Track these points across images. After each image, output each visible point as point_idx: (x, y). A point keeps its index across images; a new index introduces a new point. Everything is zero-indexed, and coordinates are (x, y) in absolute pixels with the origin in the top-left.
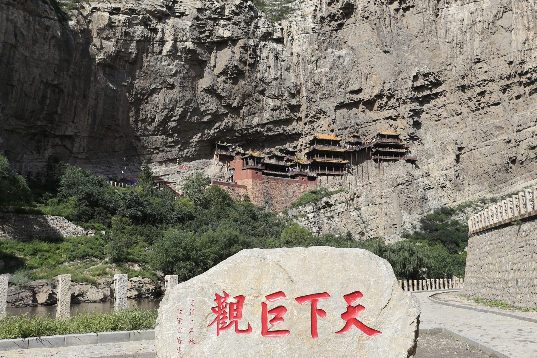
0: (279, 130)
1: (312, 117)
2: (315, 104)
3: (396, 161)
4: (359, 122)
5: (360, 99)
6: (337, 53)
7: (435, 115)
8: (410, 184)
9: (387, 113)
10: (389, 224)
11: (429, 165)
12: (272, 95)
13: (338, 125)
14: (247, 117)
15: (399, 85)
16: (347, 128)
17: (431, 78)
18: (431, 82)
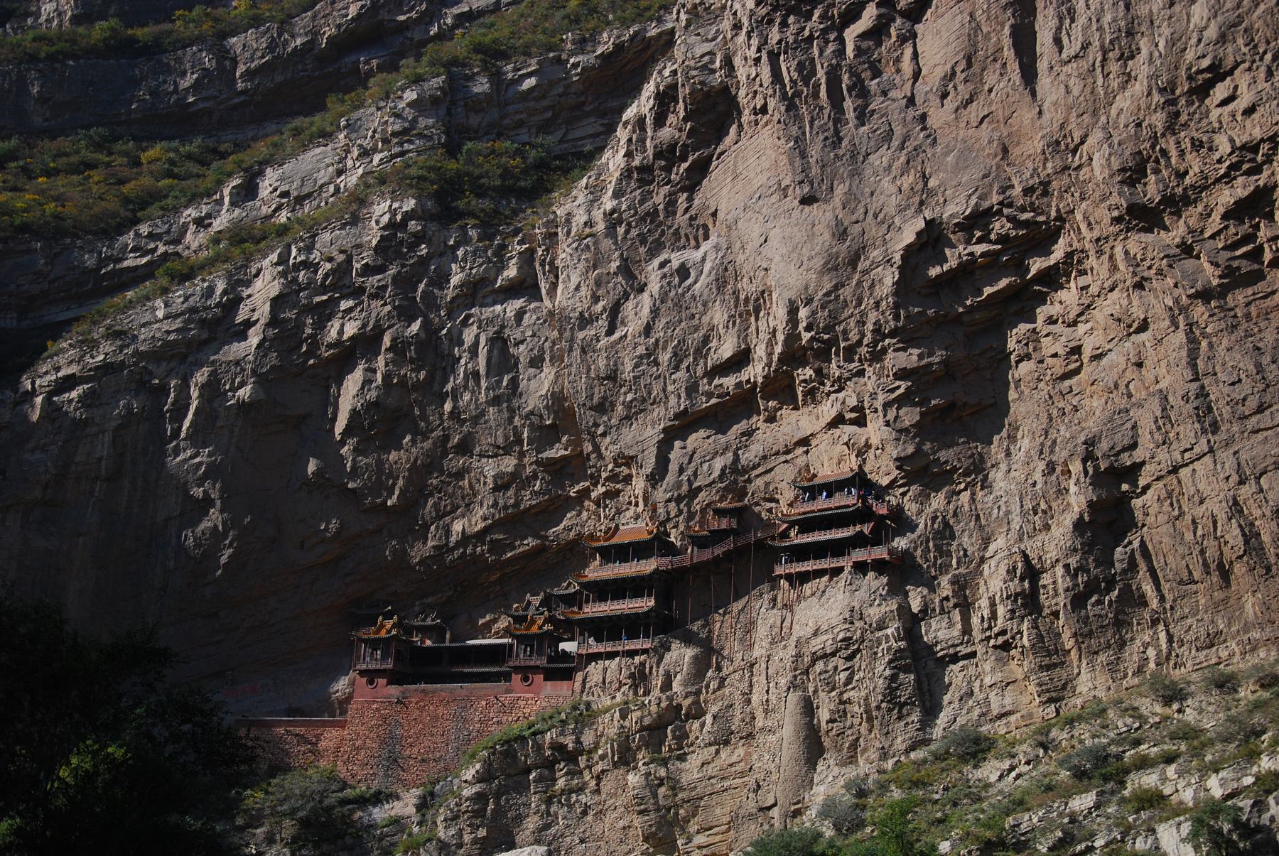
0: (525, 542)
1: (607, 479)
2: (608, 439)
3: (837, 571)
4: (747, 457)
5: (748, 381)
6: (676, 260)
7: (1055, 355)
8: (858, 650)
9: (828, 410)
10: (751, 806)
11: (986, 566)
12: (491, 448)
13: (664, 487)
14: (432, 524)
15: (849, 299)
16: (699, 489)
17: (999, 226)
18: (1003, 239)
